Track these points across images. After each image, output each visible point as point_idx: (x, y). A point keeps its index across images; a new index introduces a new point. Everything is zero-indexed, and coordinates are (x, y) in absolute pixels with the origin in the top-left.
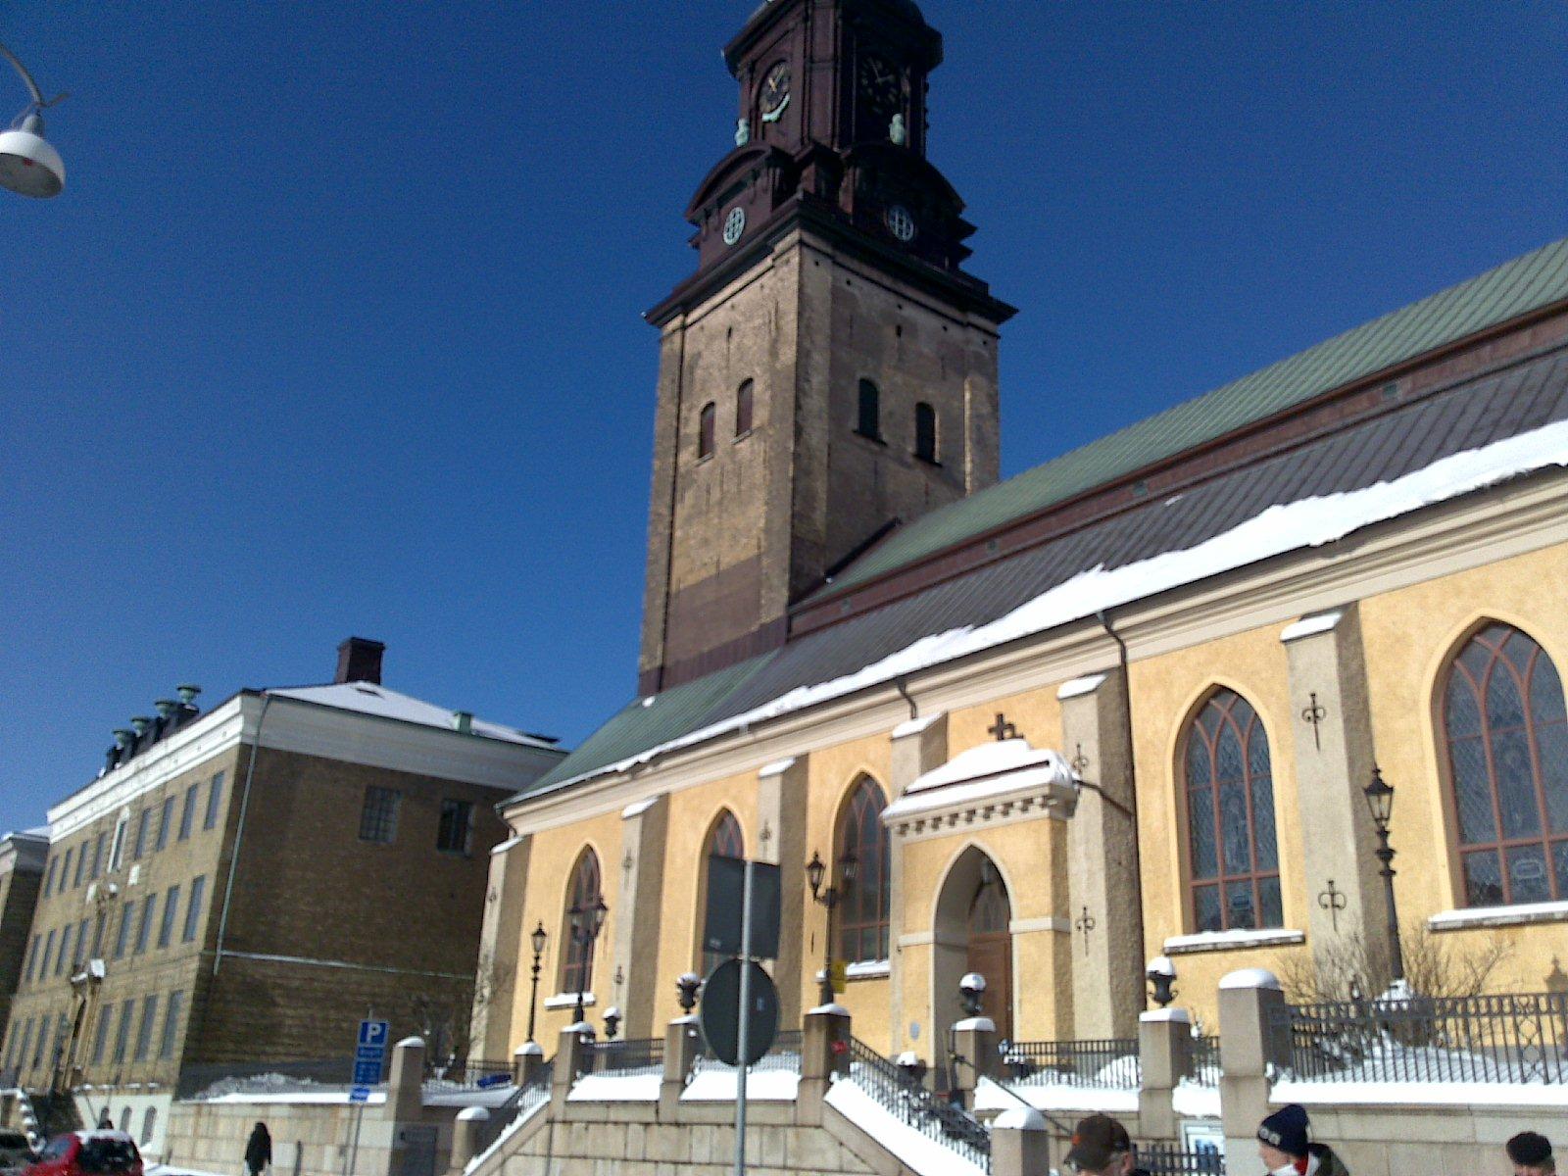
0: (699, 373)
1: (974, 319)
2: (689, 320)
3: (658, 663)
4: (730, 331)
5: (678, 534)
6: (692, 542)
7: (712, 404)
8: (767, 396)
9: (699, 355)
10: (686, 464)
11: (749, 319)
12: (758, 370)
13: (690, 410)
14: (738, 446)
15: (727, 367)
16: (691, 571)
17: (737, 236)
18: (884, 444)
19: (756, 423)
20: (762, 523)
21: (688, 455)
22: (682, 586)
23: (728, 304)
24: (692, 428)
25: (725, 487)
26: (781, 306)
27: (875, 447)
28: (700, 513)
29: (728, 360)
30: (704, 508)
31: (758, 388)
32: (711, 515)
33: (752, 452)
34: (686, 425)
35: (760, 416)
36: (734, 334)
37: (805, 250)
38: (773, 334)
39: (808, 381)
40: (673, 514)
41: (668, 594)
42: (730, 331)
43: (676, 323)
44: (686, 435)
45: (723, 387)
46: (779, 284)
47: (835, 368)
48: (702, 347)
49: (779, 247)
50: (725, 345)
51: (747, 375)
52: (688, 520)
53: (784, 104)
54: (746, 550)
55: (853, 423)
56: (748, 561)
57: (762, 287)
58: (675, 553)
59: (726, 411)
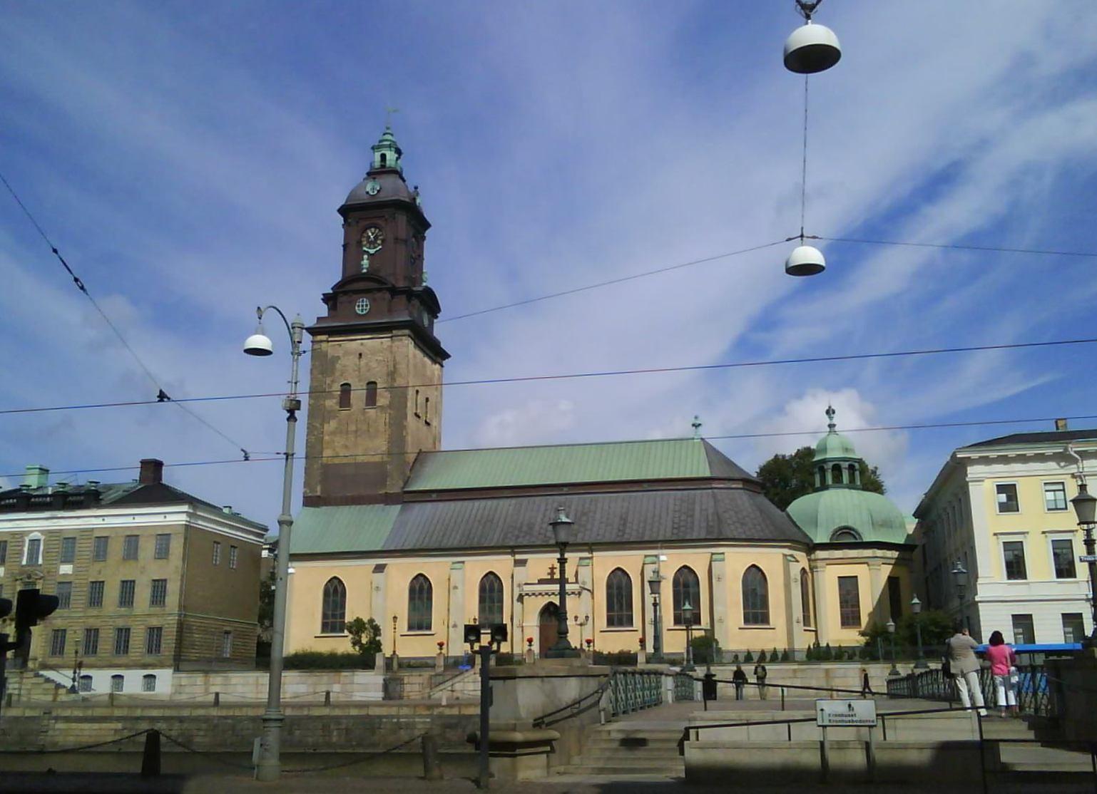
0: (338, 366)
1: (439, 360)
2: (330, 339)
3: (319, 494)
4: (360, 355)
5: (326, 438)
9: (338, 358)
10: (331, 406)
13: (333, 381)
15: (359, 372)
18: (419, 417)
19: (378, 404)
21: (331, 403)
27: (418, 419)
28: (341, 432)
29: (359, 369)
32: (350, 436)
34: (330, 386)
36: (363, 356)
37: (409, 339)
40: (323, 428)
42: (360, 355)
43: (324, 337)
45: (357, 380)
48: (340, 355)
50: (358, 360)
51: (373, 380)
52: (333, 433)
53: (378, 249)
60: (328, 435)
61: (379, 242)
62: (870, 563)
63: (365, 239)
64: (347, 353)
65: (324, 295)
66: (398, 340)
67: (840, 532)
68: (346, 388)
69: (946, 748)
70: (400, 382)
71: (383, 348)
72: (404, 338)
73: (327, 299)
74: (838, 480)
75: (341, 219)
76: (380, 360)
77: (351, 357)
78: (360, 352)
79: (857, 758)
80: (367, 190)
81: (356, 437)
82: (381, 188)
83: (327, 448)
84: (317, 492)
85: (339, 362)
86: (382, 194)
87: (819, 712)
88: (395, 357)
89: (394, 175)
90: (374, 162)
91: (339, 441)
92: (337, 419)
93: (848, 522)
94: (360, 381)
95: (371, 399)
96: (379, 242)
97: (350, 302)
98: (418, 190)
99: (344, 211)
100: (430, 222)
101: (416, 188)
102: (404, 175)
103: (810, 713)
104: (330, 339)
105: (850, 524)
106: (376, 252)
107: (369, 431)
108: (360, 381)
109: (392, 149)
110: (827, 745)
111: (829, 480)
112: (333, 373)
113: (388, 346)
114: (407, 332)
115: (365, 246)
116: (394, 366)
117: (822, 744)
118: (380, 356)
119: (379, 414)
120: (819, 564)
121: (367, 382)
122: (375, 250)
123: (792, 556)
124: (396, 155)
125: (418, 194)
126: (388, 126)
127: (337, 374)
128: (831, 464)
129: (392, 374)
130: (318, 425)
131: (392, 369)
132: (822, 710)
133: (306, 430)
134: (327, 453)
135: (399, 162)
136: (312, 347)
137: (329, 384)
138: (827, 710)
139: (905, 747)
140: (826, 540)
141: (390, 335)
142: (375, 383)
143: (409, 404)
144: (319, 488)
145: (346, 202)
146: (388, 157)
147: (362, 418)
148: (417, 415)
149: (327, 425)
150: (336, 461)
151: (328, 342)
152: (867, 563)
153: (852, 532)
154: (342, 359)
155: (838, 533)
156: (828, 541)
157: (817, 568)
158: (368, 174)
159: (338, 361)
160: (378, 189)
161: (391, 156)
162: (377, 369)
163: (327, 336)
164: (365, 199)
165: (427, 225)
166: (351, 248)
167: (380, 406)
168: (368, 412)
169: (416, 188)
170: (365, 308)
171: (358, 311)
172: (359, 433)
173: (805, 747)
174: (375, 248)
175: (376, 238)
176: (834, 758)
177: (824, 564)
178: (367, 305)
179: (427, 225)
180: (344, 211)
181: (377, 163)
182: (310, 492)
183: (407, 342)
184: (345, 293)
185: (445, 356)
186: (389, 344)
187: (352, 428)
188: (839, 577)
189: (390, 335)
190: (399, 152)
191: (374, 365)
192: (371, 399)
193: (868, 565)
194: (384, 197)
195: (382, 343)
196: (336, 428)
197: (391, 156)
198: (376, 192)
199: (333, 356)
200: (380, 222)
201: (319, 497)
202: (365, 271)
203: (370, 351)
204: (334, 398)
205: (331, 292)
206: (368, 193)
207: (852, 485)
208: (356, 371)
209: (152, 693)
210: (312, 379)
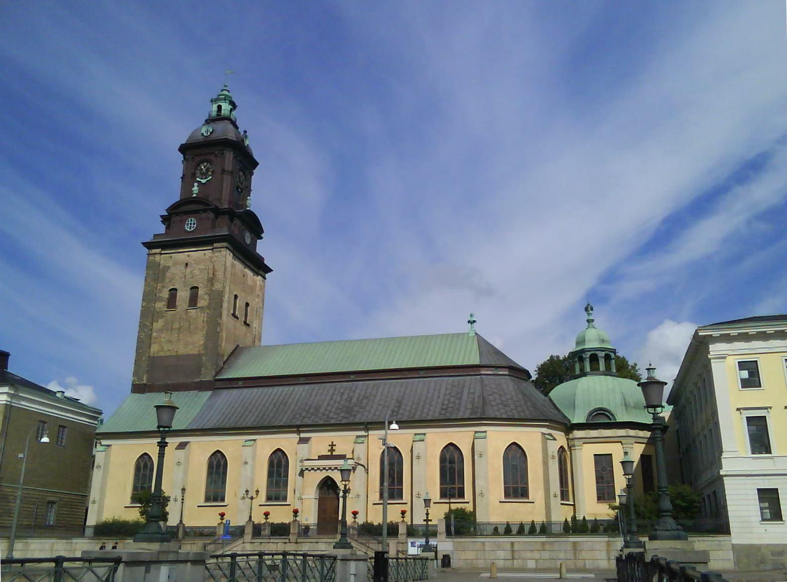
0: (168, 274)
3: (144, 382)
4: (187, 264)
5: (154, 334)
6: (162, 339)
7: (176, 290)
8: (207, 297)
9: (169, 267)
10: (160, 308)
11: (198, 263)
12: (200, 285)
13: (163, 287)
14: (188, 310)
15: (185, 278)
16: (162, 350)
17: (192, 229)
18: (237, 318)
19: (199, 305)
20: (202, 342)
21: (160, 305)
22: (155, 355)
23: (185, 253)
24: (165, 294)
25: (181, 324)
26: (216, 266)
27: (236, 319)
28: (167, 330)
29: (185, 276)
30: (170, 328)
31: (200, 292)
32: (173, 332)
33: (197, 315)
34: (161, 292)
35: (202, 302)
37: (228, 250)
38: (211, 275)
39: (224, 297)
41: (149, 356)
42: (187, 264)
44: (161, 296)
46: (216, 258)
47: (230, 292)
49: (215, 245)
52: (160, 331)
54: (193, 350)
55: (232, 312)
56: (194, 355)
57: (205, 254)
58: (152, 341)
59: (183, 295)
60: (156, 332)
61: (210, 173)
63: (198, 171)
64: (176, 263)
65: (161, 216)
66: (217, 252)
68: (174, 291)
70: (218, 286)
71: (205, 259)
72: (223, 249)
73: (165, 220)
75: (181, 156)
76: (203, 269)
77: (178, 267)
78: (186, 262)
80: (202, 132)
81: (179, 334)
82: (213, 130)
83: (154, 343)
84: (143, 380)
85: (169, 271)
86: (212, 136)
88: (214, 265)
89: (226, 121)
90: (212, 111)
91: (164, 337)
92: (164, 318)
94: (185, 286)
95: (193, 301)
96: (210, 173)
97: (181, 221)
98: (247, 134)
99: (183, 149)
100: (258, 161)
101: (245, 132)
102: (237, 124)
104: (162, 252)
106: (206, 181)
107: (189, 328)
108: (185, 286)
109: (227, 101)
112: (163, 281)
113: (210, 257)
114: (225, 244)
115: (198, 177)
116: (213, 274)
118: (202, 265)
119: (199, 313)
121: (191, 287)
122: (206, 180)
124: (230, 107)
125: (246, 137)
126: (226, 84)
127: (167, 280)
129: (211, 280)
130: (148, 324)
131: (212, 276)
133: (138, 328)
134: (154, 348)
135: (233, 113)
136: (148, 259)
137: (159, 289)
141: (211, 248)
142: (197, 288)
143: (225, 305)
144: (145, 378)
145: (187, 141)
146: (223, 108)
147: (185, 317)
148: (234, 315)
149: (156, 323)
150: (161, 354)
151: (161, 254)
154: (171, 268)
158: (206, 121)
159: (168, 270)
160: (211, 131)
161: (226, 107)
162: (200, 276)
163: (160, 250)
164: (201, 138)
165: (255, 164)
166: (188, 179)
167: (199, 307)
168: (191, 312)
169: (245, 132)
170: (192, 226)
171: (187, 229)
172: (181, 330)
174: (206, 178)
175: (207, 170)
178: (194, 224)
179: (255, 164)
180: (183, 149)
181: (214, 114)
182: (138, 381)
183: (225, 253)
184: (177, 214)
185: (268, 270)
186: (210, 255)
187: (176, 325)
189: (211, 248)
190: (234, 106)
191: (197, 272)
192: (193, 301)
194: (215, 136)
195: (205, 254)
196: (164, 326)
197: (226, 107)
198: (209, 134)
199: (164, 266)
200: (212, 158)
201: (145, 384)
202: (194, 195)
203: (195, 261)
204: (163, 301)
205: (167, 214)
206: (203, 134)
208: (182, 278)
209: (204, 542)
210: (145, 286)
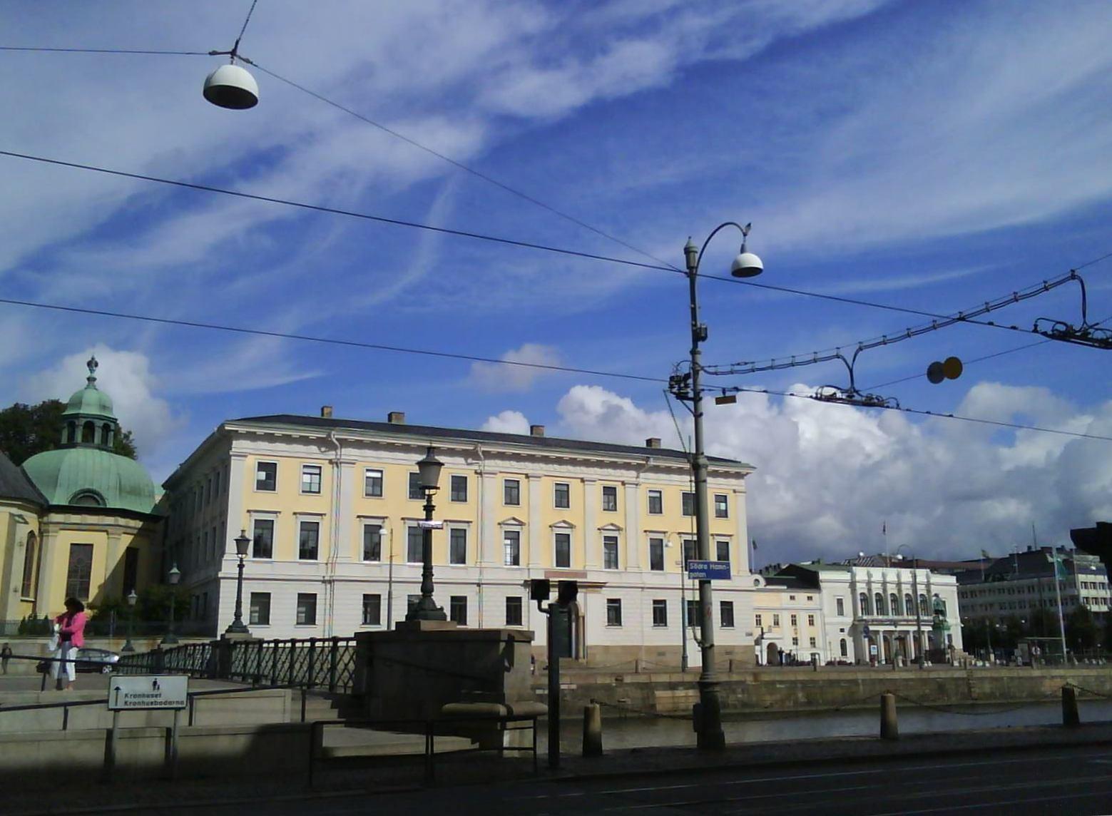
62: (110, 530)
67: (82, 495)
69: (265, 734)
74: (88, 440)
79: (153, 750)
87: (113, 692)
93: (92, 485)
103: (100, 694)
105: (95, 487)
110: (116, 735)
111: (79, 438)
117: (110, 733)
120: (51, 528)
123: (20, 516)
128: (83, 421)
132: (117, 689)
138: (124, 690)
139: (214, 733)
140: (64, 502)
152: (106, 531)
153: (96, 496)
155: (79, 496)
156: (67, 504)
157: (48, 532)
173: (86, 737)
176: (123, 751)
177: (57, 528)
188: (72, 544)
193: (108, 534)
207: (103, 447)
